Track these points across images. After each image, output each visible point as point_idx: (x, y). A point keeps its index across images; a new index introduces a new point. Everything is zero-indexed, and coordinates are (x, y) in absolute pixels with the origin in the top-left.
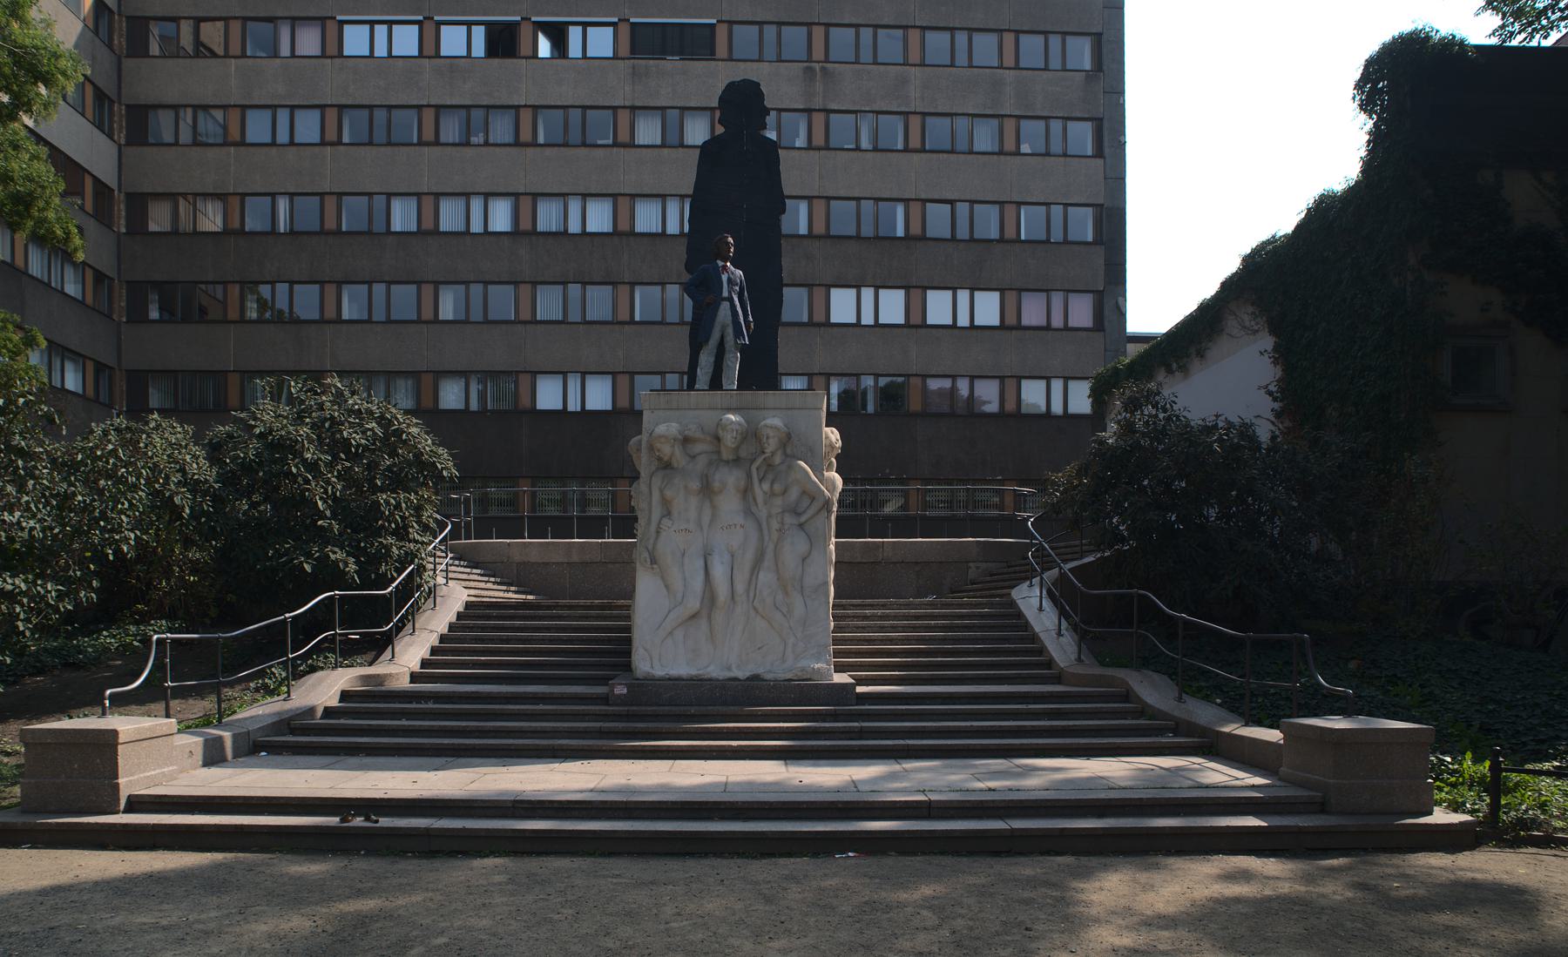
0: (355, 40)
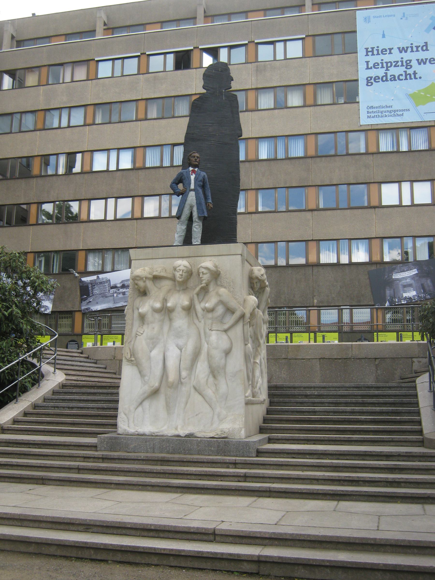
0: (105, 70)
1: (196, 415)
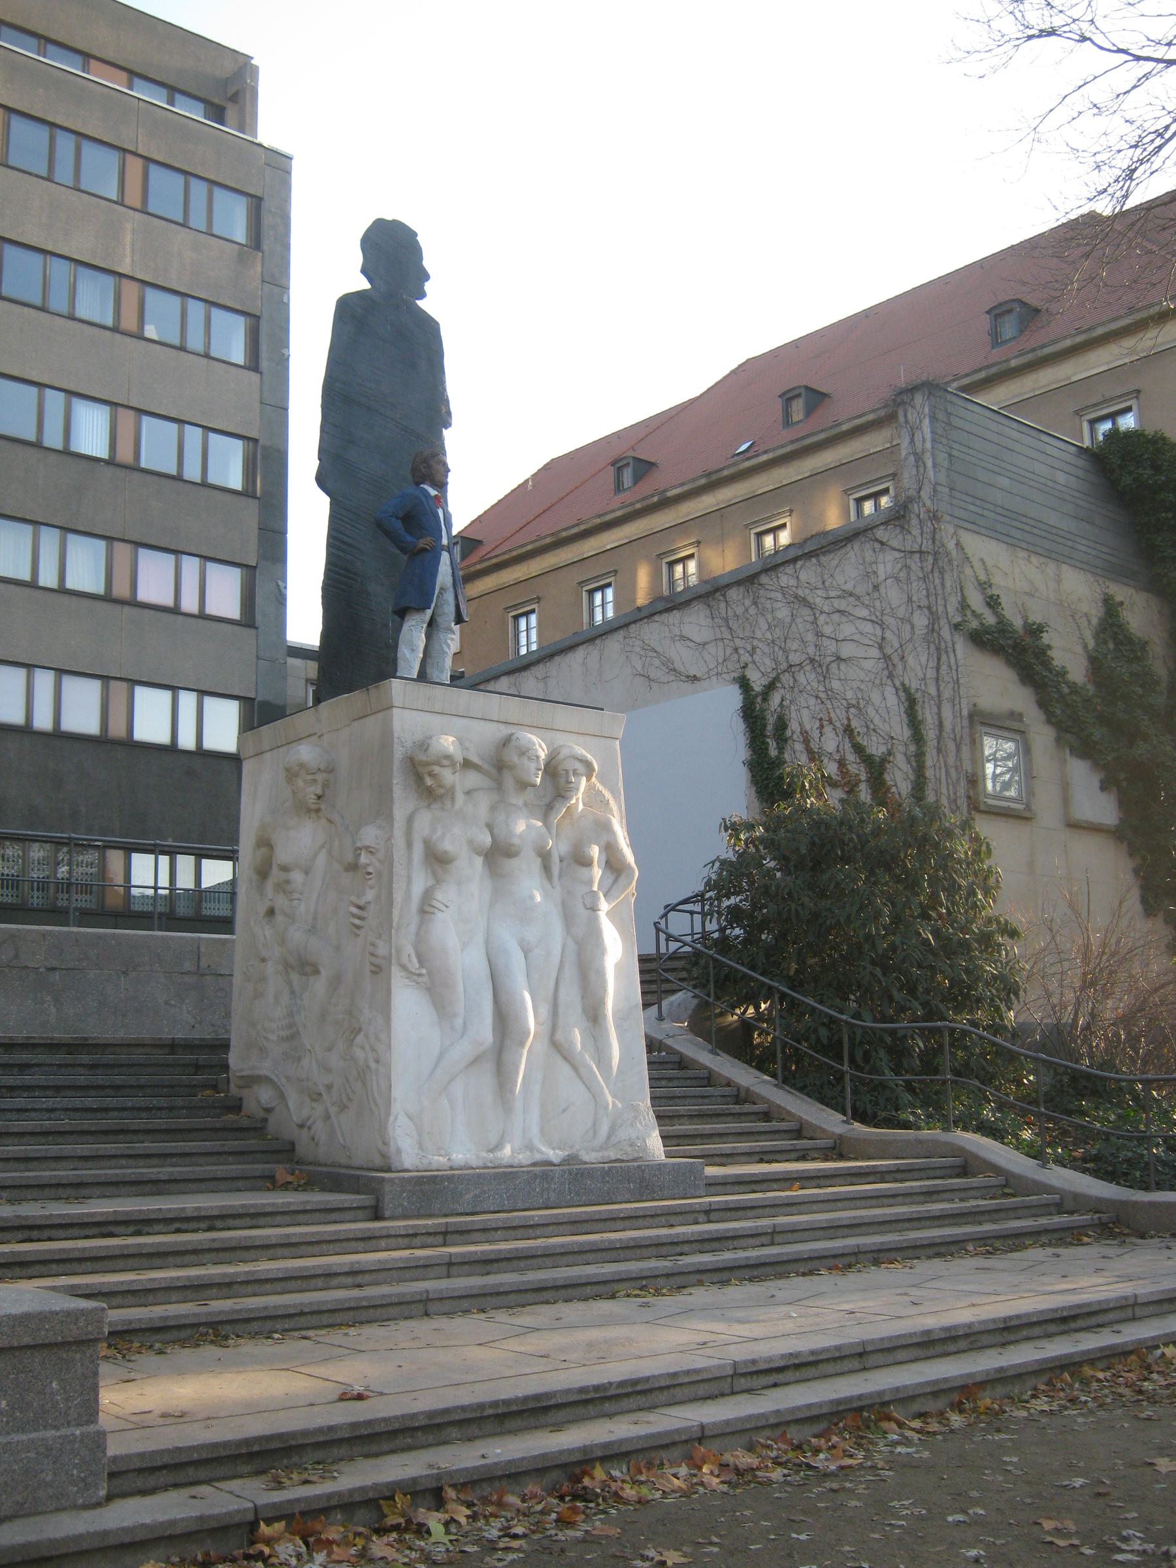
1: (564, 1111)
